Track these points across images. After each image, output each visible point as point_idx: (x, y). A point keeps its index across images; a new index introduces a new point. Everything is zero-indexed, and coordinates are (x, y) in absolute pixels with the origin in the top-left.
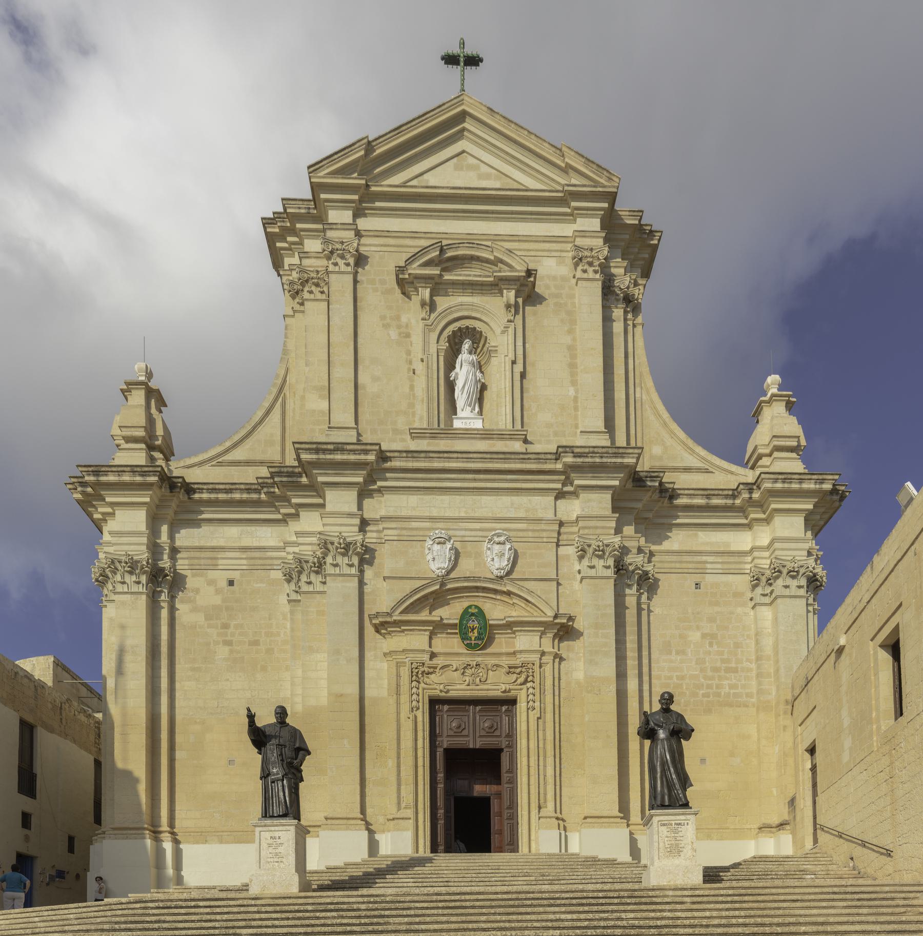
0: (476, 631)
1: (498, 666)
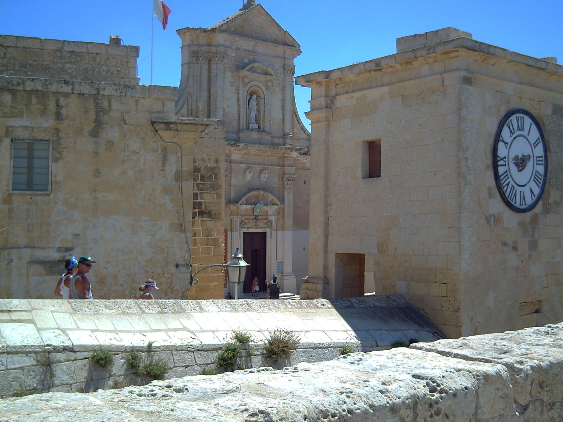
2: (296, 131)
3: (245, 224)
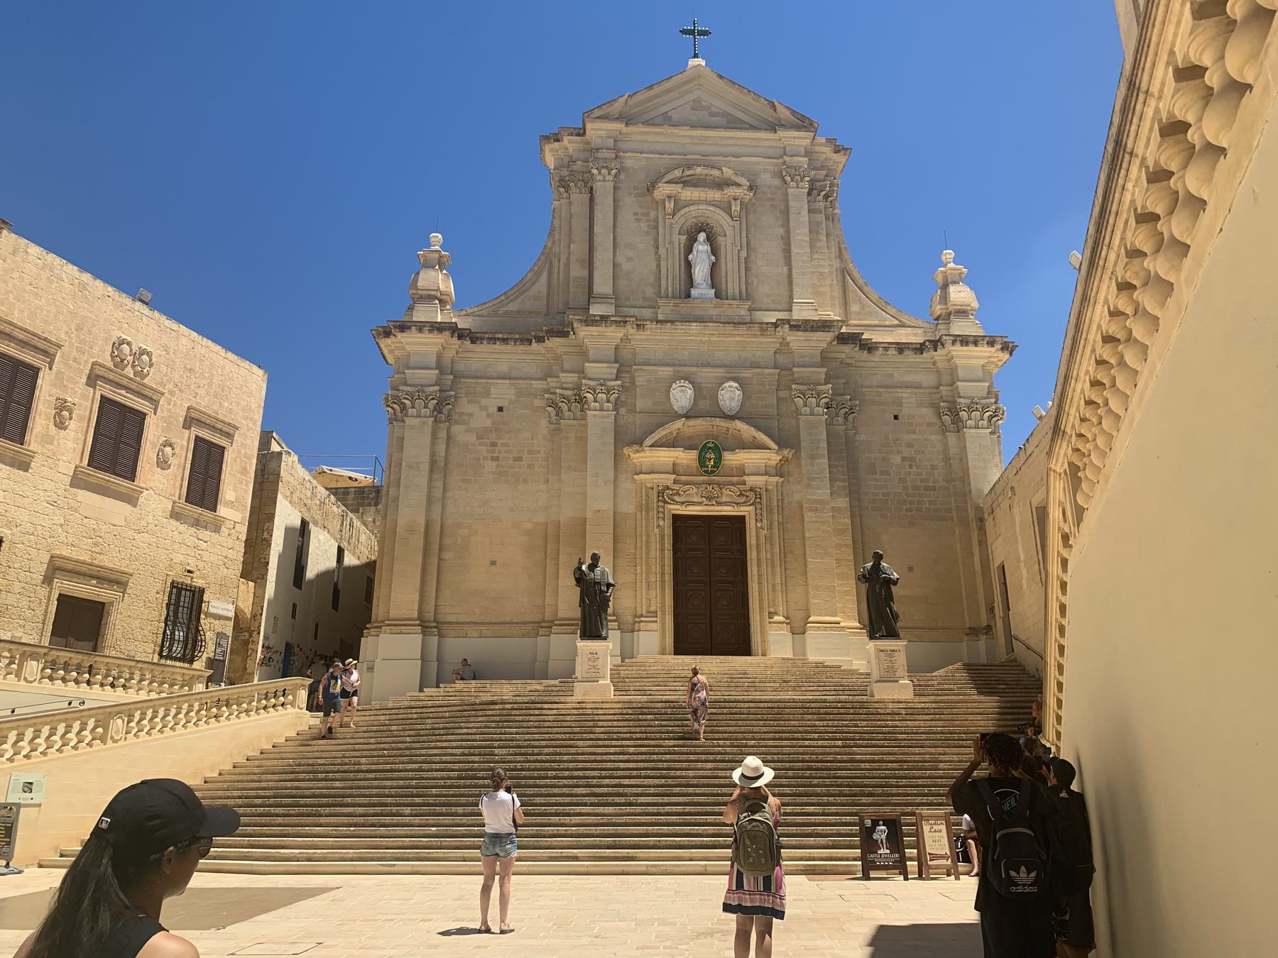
0: (712, 461)
3: (675, 495)
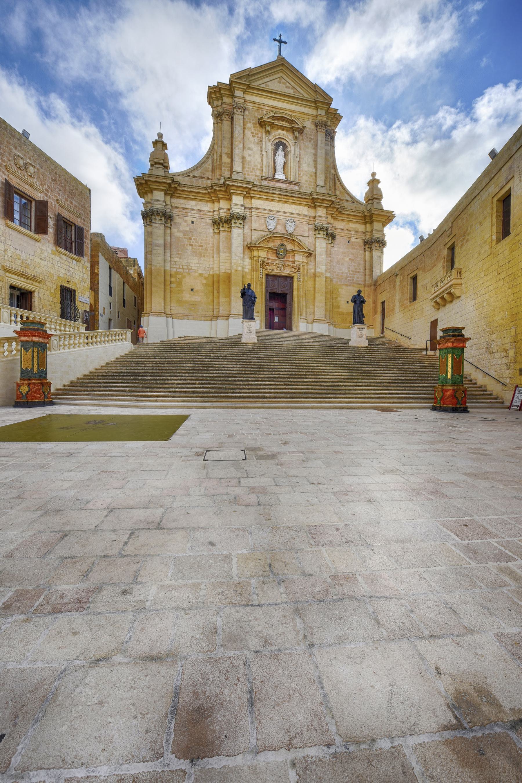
1: (289, 265)
2: (338, 193)
